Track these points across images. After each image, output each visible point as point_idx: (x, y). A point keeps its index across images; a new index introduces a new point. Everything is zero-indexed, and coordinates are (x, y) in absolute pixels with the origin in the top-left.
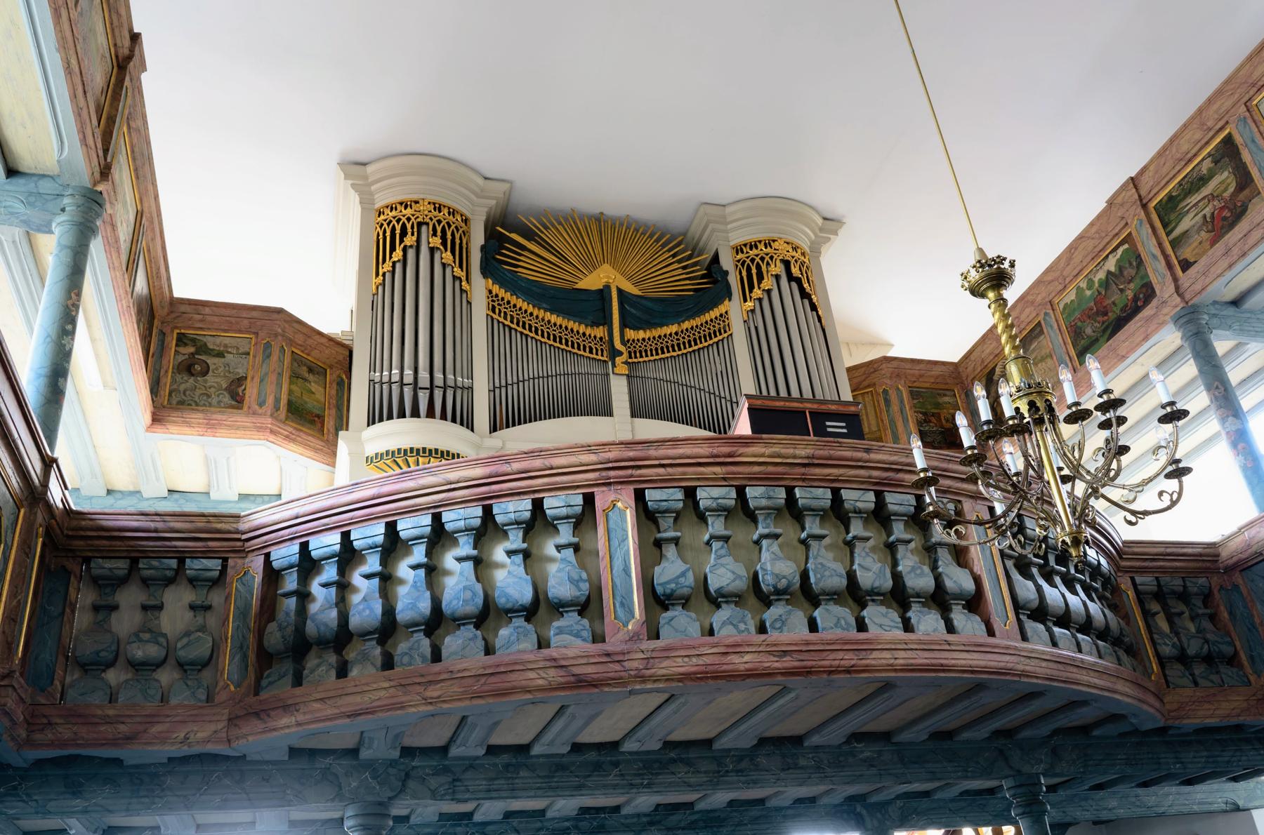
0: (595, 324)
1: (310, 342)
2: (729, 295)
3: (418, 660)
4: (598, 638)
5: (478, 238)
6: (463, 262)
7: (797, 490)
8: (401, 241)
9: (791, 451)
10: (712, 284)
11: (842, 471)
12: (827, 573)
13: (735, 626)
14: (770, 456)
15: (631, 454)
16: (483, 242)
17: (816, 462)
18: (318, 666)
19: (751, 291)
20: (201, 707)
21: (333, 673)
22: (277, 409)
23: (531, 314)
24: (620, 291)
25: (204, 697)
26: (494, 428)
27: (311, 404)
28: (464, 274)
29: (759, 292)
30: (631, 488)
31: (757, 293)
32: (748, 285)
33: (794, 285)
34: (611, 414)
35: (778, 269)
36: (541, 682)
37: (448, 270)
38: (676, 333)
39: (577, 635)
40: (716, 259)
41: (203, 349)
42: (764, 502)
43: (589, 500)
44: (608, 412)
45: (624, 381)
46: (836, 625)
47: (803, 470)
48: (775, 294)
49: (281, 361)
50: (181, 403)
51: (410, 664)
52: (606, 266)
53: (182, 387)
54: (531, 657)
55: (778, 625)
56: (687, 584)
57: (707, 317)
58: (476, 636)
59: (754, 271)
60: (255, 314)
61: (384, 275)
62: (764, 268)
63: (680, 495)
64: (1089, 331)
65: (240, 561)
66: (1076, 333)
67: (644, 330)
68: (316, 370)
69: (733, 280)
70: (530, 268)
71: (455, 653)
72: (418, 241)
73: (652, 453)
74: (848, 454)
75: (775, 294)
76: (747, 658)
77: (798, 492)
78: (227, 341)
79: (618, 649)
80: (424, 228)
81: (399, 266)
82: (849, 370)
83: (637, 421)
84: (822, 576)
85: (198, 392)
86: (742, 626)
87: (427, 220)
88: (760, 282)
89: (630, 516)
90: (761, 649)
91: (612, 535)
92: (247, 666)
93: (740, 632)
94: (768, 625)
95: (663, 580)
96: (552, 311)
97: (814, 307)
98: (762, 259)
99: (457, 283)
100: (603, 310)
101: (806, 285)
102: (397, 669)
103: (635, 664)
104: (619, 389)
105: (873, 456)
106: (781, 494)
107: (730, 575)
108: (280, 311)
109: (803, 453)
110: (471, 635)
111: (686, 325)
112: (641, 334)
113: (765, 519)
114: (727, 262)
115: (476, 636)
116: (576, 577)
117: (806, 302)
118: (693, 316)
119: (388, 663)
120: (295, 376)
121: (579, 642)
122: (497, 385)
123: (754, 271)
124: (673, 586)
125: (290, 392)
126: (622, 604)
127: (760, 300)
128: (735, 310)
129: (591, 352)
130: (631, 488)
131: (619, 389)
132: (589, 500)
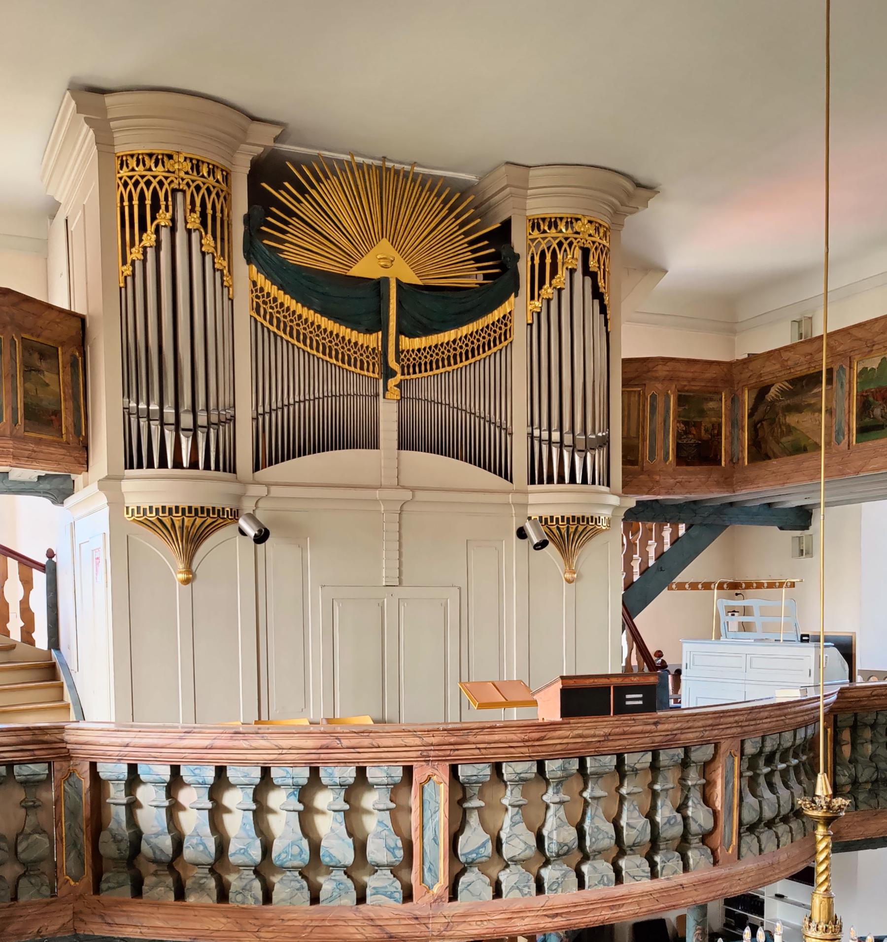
0: (369, 331)
1: (40, 322)
2: (515, 289)
3: (251, 901)
4: (408, 897)
5: (240, 205)
6: (226, 252)
7: (588, 759)
8: (154, 218)
10: (501, 279)
12: (600, 837)
13: (520, 890)
15: (452, 740)
16: (246, 211)
18: (156, 885)
20: (48, 904)
21: (172, 895)
23: (300, 316)
24: (399, 283)
25: (48, 893)
27: (46, 399)
28: (225, 263)
29: (550, 290)
30: (447, 764)
31: (548, 291)
32: (539, 279)
34: (377, 447)
35: (574, 258)
36: (359, 937)
37: (208, 258)
38: (454, 341)
39: (391, 897)
40: (507, 225)
43: (408, 771)
44: (374, 444)
45: (395, 407)
46: (599, 882)
48: (565, 294)
51: (243, 903)
52: (385, 242)
54: (351, 915)
55: (554, 887)
56: (486, 854)
58: (302, 887)
61: (133, 262)
62: (560, 257)
63: (488, 771)
64: (878, 412)
65: (65, 764)
66: (865, 407)
68: (47, 353)
69: (523, 268)
70: (299, 250)
71: (283, 900)
72: (173, 220)
73: (471, 739)
75: (565, 294)
76: (527, 921)
79: (425, 914)
80: (179, 196)
81: (150, 253)
82: (625, 361)
83: (403, 452)
86: (526, 890)
87: (183, 186)
88: (552, 277)
89: (443, 790)
90: (539, 913)
91: (426, 806)
92: (83, 864)
93: (524, 895)
94: (546, 885)
95: (466, 851)
96: (323, 314)
97: (603, 310)
98: (560, 244)
99: (218, 274)
100: (379, 312)
101: (601, 283)
102: (231, 905)
103: (438, 926)
104: (388, 416)
105: (660, 727)
106: (575, 765)
107: (523, 846)
110: (298, 885)
112: (418, 343)
115: (302, 887)
116: (393, 845)
117: (596, 302)
119: (223, 895)
120: (29, 369)
121: (391, 902)
122: (261, 410)
124: (474, 855)
125: (26, 393)
126: (430, 869)
128: (519, 308)
129: (362, 368)
130: (447, 764)
131: (388, 416)
132: (408, 771)
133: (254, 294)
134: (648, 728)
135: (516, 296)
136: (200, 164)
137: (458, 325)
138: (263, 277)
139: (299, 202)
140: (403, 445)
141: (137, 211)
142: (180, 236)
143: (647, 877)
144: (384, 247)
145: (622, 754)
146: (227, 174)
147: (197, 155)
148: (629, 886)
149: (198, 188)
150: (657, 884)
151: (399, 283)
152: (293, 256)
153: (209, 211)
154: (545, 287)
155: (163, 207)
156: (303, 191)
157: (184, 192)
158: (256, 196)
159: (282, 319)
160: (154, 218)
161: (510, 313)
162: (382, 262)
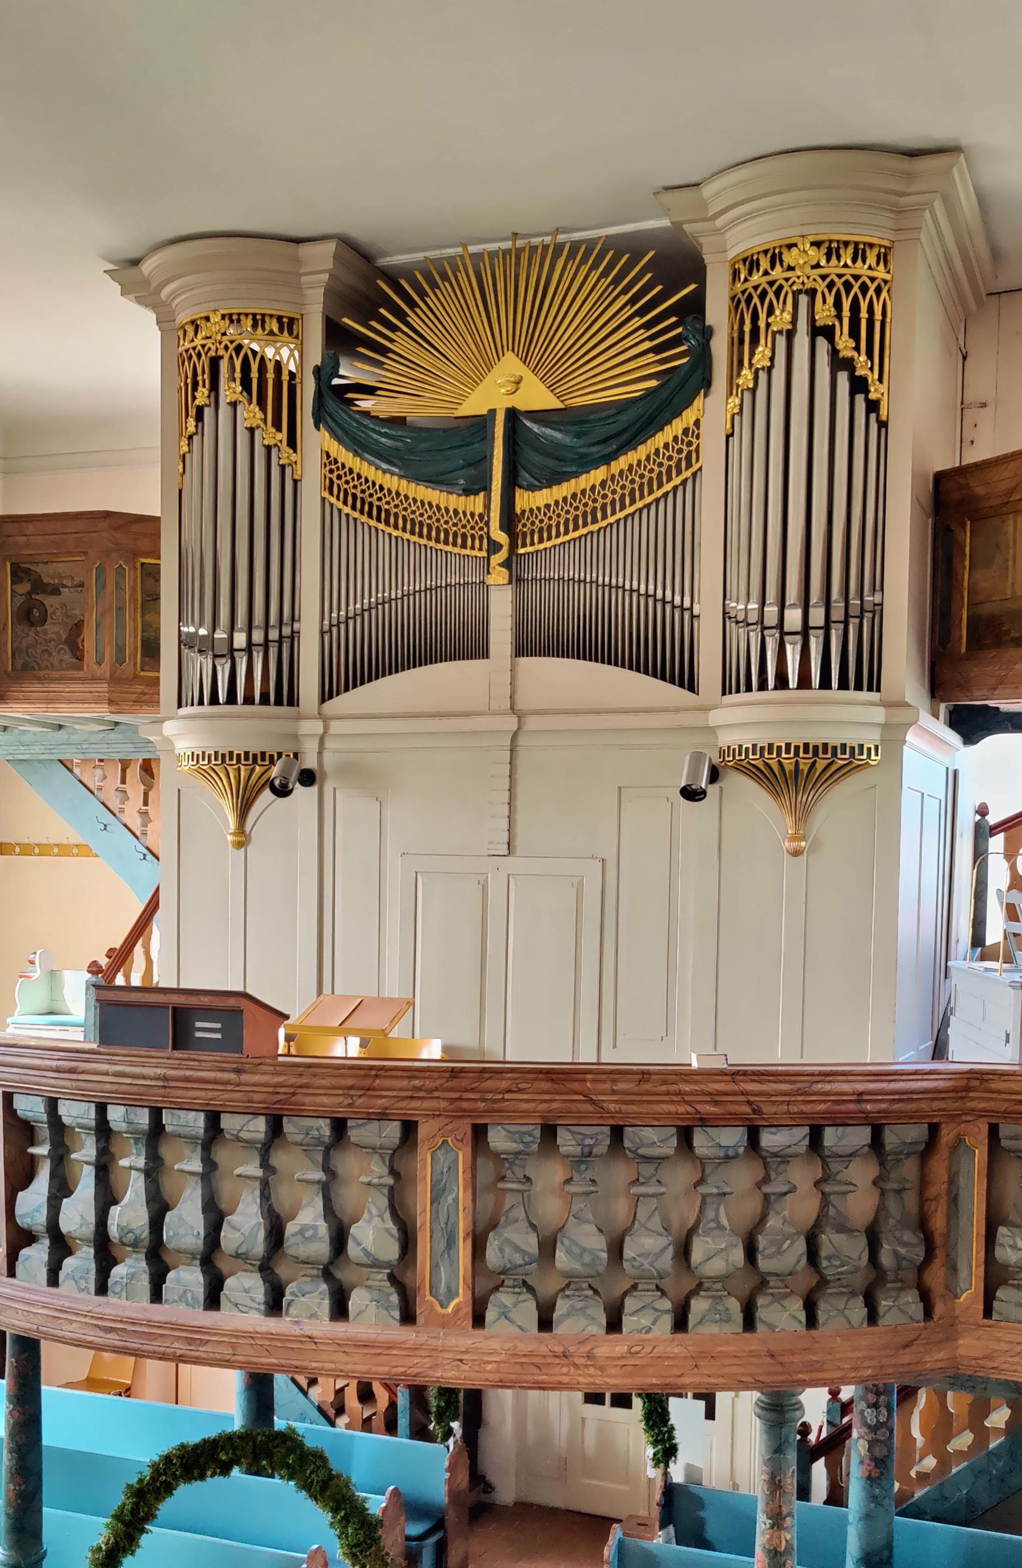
0: (468, 492)
2: (706, 383)
22: (120, 660)
26: (326, 695)
28: (283, 436)
41: (39, 586)
49: (120, 588)
50: (25, 667)
53: (24, 643)
69: (720, 348)
78: (61, 568)
85: (40, 648)
88: (752, 355)
111: (622, 463)
112: (542, 498)
118: (631, 443)
127: (754, 391)
133: (328, 468)
135: (706, 396)
137: (607, 459)
139: (394, 328)
140: (523, 647)
142: (224, 411)
144: (511, 364)
151: (512, 414)
154: (744, 372)
155: (201, 383)
159: (359, 495)
160: (194, 398)
162: (506, 387)
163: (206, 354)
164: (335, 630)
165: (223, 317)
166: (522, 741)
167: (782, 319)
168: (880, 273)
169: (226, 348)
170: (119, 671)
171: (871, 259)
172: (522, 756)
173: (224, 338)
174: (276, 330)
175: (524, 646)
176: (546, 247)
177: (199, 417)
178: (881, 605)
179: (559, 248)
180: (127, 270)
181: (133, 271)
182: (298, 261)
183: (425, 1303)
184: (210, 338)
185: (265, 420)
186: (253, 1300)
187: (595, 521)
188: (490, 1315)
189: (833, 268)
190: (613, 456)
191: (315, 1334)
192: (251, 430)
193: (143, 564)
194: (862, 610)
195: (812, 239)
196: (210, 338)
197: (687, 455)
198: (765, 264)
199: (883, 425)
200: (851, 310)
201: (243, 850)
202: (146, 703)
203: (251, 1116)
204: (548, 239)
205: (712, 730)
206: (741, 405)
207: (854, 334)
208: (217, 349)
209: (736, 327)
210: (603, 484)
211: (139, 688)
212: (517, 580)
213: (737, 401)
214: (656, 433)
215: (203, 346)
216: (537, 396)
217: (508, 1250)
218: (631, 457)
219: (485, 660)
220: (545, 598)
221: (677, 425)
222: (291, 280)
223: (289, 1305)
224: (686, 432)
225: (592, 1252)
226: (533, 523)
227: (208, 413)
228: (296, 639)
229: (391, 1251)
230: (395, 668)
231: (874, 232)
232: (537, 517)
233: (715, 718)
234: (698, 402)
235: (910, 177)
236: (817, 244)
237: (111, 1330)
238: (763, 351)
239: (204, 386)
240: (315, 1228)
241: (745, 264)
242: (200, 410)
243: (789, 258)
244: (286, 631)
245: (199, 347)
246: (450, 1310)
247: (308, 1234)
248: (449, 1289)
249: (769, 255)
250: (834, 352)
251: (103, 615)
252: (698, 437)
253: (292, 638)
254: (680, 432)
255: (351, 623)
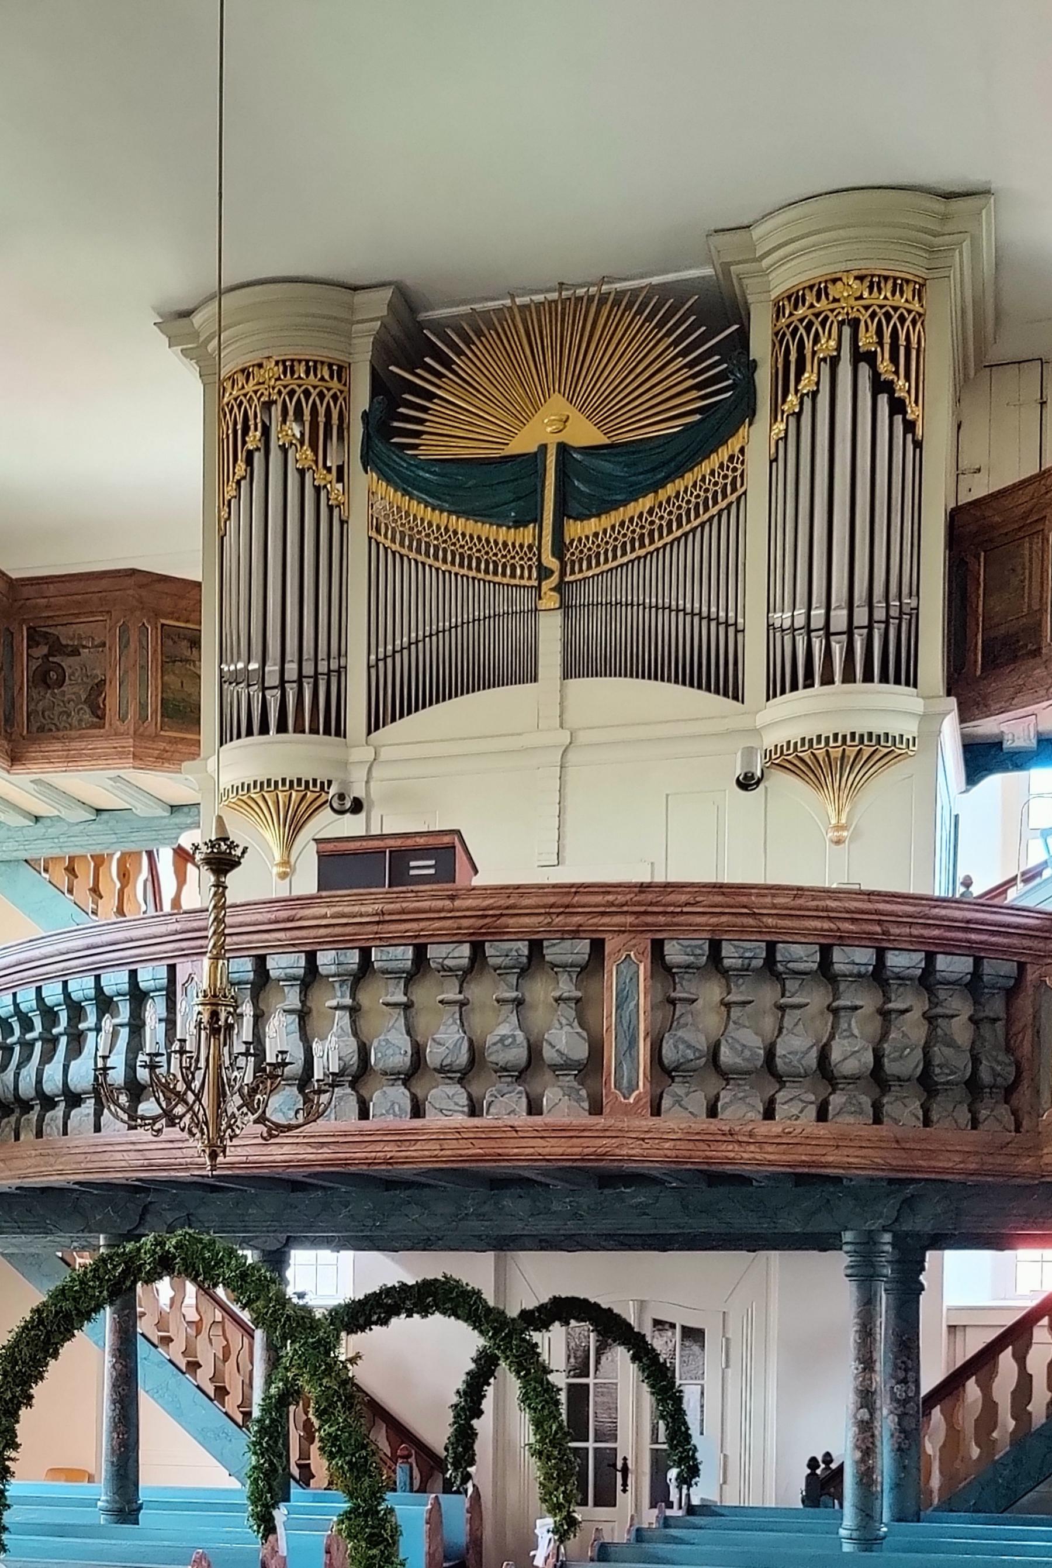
9: (356, 909)
11: (422, 924)
12: (390, 1052)
14: (332, 917)
17: (387, 918)
19: (784, 401)
33: (864, 369)
42: (333, 969)
47: (375, 928)
57: (705, 467)
59: (793, 357)
60: (104, 583)
67: (598, 516)
74: (426, 905)
77: (374, 954)
84: (384, 1055)
105: (458, 903)
108: (133, 572)
109: (369, 909)
111: (670, 489)
113: (341, 986)
114: (761, 345)
118: (679, 472)
123: (793, 357)
134: (440, 904)
135: (750, 425)
136: (296, 363)
137: (656, 487)
138: (384, 484)
141: (238, 438)
142: (275, 455)
143: (463, 1112)
145: (425, 945)
146: (340, 368)
147: (289, 353)
148: (433, 1120)
149: (292, 393)
150: (476, 1121)
151: (563, 449)
152: (431, 449)
153: (322, 419)
155: (252, 427)
156: (447, 363)
157: (275, 402)
158: (379, 384)
160: (244, 443)
161: (742, 451)
163: (259, 399)
164: (381, 664)
165: (277, 363)
166: (571, 756)
167: (827, 345)
168: (916, 306)
169: (280, 393)
170: (142, 729)
171: (908, 294)
172: (571, 772)
173: (278, 383)
174: (327, 377)
175: (577, 665)
176: (591, 299)
177: (249, 461)
178: (917, 609)
179: (603, 299)
180: (176, 321)
181: (185, 320)
182: (351, 308)
183: (611, 1093)
184: (263, 383)
185: (316, 462)
186: (456, 1104)
187: (642, 545)
188: (666, 1103)
189: (877, 299)
190: (661, 484)
191: (516, 1124)
192: (302, 472)
193: (163, 625)
194: (901, 612)
195: (856, 273)
196: (263, 383)
197: (734, 481)
198: (810, 298)
199: (918, 445)
200: (891, 337)
201: (288, 880)
202: (168, 760)
203: (453, 946)
204: (593, 290)
205: (757, 732)
206: (786, 430)
207: (894, 359)
208: (270, 394)
209: (780, 360)
210: (651, 512)
211: (162, 745)
212: (565, 606)
213: (783, 427)
214: (702, 461)
215: (256, 392)
216: (585, 433)
217: (681, 1047)
218: (679, 484)
219: (533, 684)
220: (593, 626)
221: (723, 452)
222: (341, 327)
223: (490, 1105)
224: (731, 458)
225: (751, 1049)
226: (581, 552)
227: (258, 457)
228: (343, 674)
229: (581, 1052)
230: (441, 697)
231: (910, 267)
232: (585, 546)
233: (761, 719)
234: (743, 431)
235: (945, 218)
236: (860, 278)
237: (323, 1144)
238: (807, 382)
239: (256, 429)
240: (514, 1036)
241: (790, 302)
242: (250, 455)
243: (834, 291)
244: (334, 666)
245: (251, 393)
246: (631, 1101)
247: (507, 1043)
248: (630, 1081)
249: (815, 289)
250: (876, 375)
251: (126, 672)
252: (743, 463)
253: (339, 672)
254: (726, 458)
255: (398, 656)
